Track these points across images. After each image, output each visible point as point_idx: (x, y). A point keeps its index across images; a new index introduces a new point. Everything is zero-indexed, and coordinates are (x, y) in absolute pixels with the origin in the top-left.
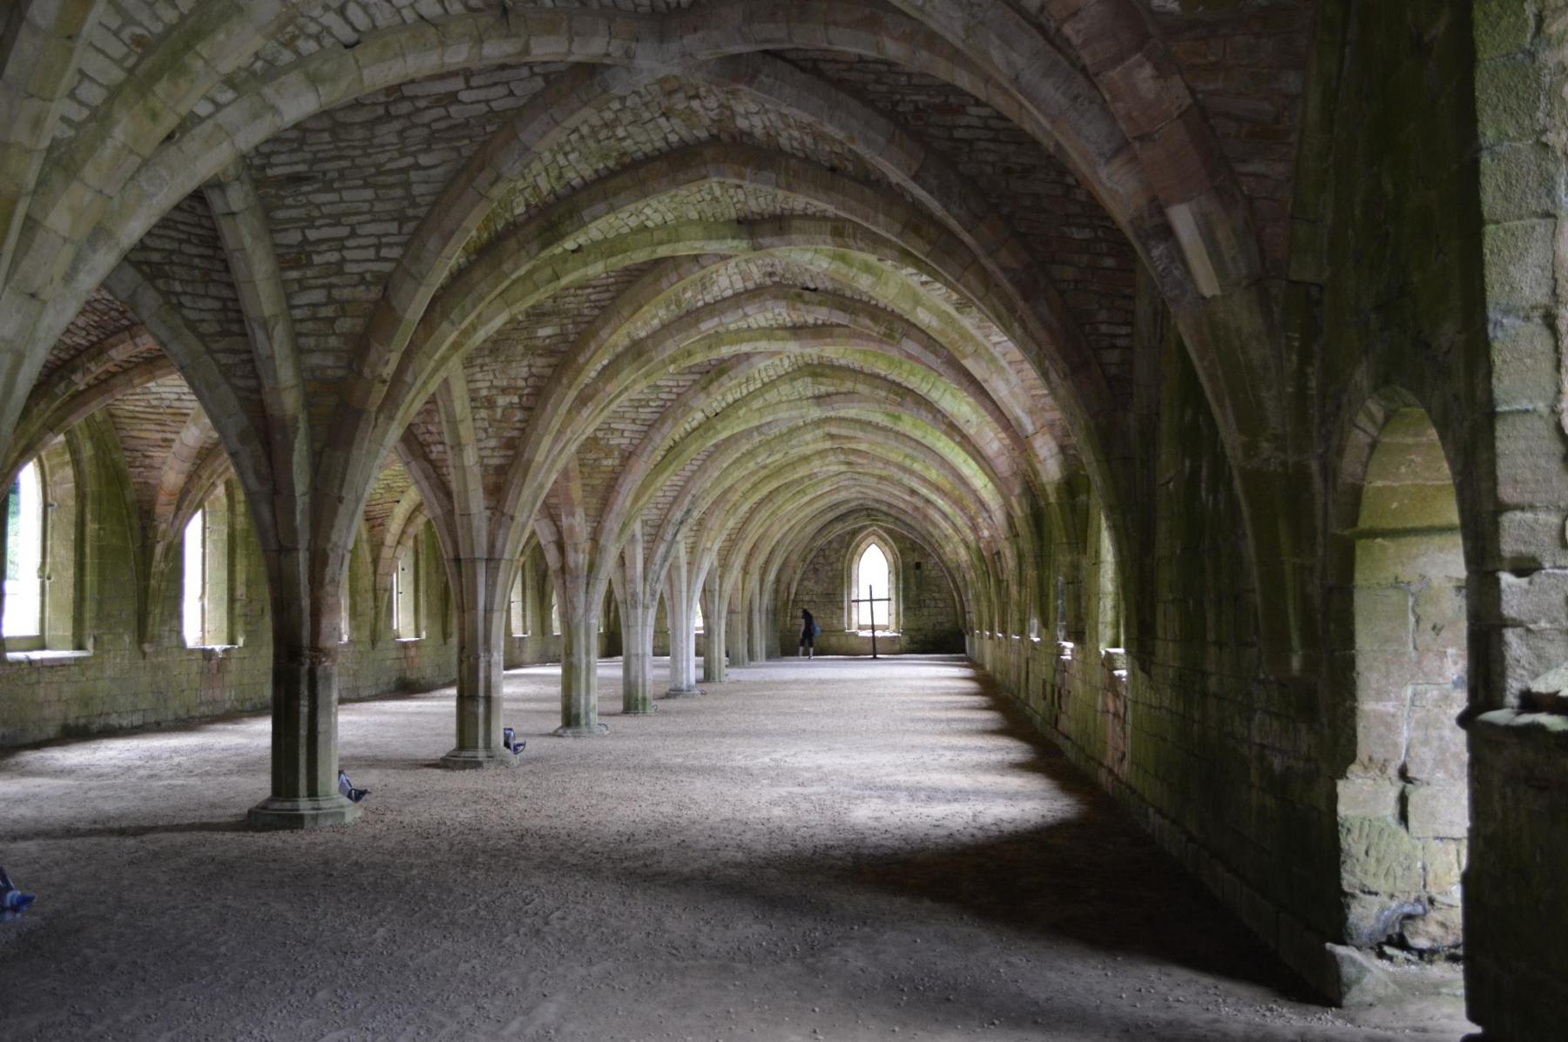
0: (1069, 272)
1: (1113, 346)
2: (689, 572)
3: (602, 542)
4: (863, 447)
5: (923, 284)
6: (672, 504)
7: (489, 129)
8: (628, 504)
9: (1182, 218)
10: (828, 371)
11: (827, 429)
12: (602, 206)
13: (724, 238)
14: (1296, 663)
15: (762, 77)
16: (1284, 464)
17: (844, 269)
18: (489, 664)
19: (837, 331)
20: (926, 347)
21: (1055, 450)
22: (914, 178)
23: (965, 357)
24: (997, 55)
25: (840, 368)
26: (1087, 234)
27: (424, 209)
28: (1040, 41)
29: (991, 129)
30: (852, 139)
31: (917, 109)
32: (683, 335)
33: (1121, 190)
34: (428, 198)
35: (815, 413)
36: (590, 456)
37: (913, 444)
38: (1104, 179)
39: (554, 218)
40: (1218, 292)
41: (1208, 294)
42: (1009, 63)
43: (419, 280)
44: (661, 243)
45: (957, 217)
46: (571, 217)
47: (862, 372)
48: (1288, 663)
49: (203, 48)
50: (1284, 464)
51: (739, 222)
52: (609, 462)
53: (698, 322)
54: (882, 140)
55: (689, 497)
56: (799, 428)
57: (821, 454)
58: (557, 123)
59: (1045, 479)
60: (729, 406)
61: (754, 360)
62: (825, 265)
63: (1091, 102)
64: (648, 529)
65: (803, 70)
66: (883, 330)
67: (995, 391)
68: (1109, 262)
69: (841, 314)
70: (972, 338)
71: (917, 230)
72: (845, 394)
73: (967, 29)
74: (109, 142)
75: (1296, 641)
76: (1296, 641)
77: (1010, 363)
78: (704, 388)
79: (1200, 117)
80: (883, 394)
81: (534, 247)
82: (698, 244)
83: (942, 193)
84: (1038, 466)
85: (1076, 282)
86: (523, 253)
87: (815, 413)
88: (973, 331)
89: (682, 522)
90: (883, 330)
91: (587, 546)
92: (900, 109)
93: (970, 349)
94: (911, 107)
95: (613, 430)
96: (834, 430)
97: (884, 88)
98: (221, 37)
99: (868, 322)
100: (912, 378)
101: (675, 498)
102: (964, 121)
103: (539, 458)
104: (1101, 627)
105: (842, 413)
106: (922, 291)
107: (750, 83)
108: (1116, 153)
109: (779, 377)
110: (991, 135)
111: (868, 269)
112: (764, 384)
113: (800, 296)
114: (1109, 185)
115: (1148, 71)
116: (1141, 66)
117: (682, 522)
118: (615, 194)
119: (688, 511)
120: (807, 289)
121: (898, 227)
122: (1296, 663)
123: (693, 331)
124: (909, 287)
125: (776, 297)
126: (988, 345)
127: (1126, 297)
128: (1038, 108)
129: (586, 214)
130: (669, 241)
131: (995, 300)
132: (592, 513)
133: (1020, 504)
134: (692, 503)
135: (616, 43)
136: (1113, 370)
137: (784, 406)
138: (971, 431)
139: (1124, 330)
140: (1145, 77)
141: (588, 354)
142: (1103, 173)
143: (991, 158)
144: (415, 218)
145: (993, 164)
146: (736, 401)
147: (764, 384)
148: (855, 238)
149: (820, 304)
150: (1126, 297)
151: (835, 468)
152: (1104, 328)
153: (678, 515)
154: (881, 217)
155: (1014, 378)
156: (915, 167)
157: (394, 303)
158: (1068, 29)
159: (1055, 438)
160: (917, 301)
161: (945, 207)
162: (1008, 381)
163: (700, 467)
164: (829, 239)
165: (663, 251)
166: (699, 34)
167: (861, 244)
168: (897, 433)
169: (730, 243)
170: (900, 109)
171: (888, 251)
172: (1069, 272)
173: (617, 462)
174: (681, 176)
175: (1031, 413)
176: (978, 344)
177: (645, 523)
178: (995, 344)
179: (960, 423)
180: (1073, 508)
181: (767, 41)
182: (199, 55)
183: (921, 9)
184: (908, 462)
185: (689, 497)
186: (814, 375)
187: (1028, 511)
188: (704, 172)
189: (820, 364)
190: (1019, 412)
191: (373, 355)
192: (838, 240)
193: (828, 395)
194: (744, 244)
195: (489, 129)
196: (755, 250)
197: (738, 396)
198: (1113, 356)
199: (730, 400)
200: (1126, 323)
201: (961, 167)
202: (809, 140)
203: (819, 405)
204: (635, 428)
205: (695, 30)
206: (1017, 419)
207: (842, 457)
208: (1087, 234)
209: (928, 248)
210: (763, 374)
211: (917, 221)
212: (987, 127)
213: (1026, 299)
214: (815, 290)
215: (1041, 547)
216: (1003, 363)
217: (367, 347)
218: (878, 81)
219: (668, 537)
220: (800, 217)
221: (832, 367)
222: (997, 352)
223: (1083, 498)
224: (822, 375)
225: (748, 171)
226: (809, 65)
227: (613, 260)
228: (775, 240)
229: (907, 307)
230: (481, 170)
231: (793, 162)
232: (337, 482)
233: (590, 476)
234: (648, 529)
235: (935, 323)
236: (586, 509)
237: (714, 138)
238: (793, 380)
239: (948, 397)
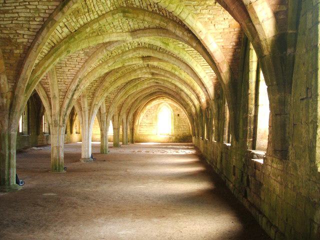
2: (89, 113)
3: (16, 93)
6: (71, 82)
10: (131, 10)
36: (7, 48)
52: (18, 51)
55: (78, 79)
56: (127, 51)
57: (141, 68)
60: (82, 26)
64: (61, 93)
89: (75, 90)
91: (9, 95)
95: (19, 34)
100: (171, 5)
101: (73, 80)
109: (107, 13)
112: (99, 16)
117: (75, 90)
119: (78, 86)
132: (11, 77)
134: (80, 82)
137: (115, 34)
146: (85, 24)
147: (99, 16)
151: (147, 76)
153: (73, 87)
163: (82, 66)
173: (22, 51)
177: (60, 90)
184: (173, 71)
185: (78, 79)
197: (85, 21)
199: (82, 23)
203: (132, 36)
204: (30, 33)
207: (148, 70)
210: (97, 9)
219: (70, 97)
224: (128, 12)
233: (9, 59)
234: (61, 93)
236: (8, 76)
238: (113, 14)
239: (190, 17)
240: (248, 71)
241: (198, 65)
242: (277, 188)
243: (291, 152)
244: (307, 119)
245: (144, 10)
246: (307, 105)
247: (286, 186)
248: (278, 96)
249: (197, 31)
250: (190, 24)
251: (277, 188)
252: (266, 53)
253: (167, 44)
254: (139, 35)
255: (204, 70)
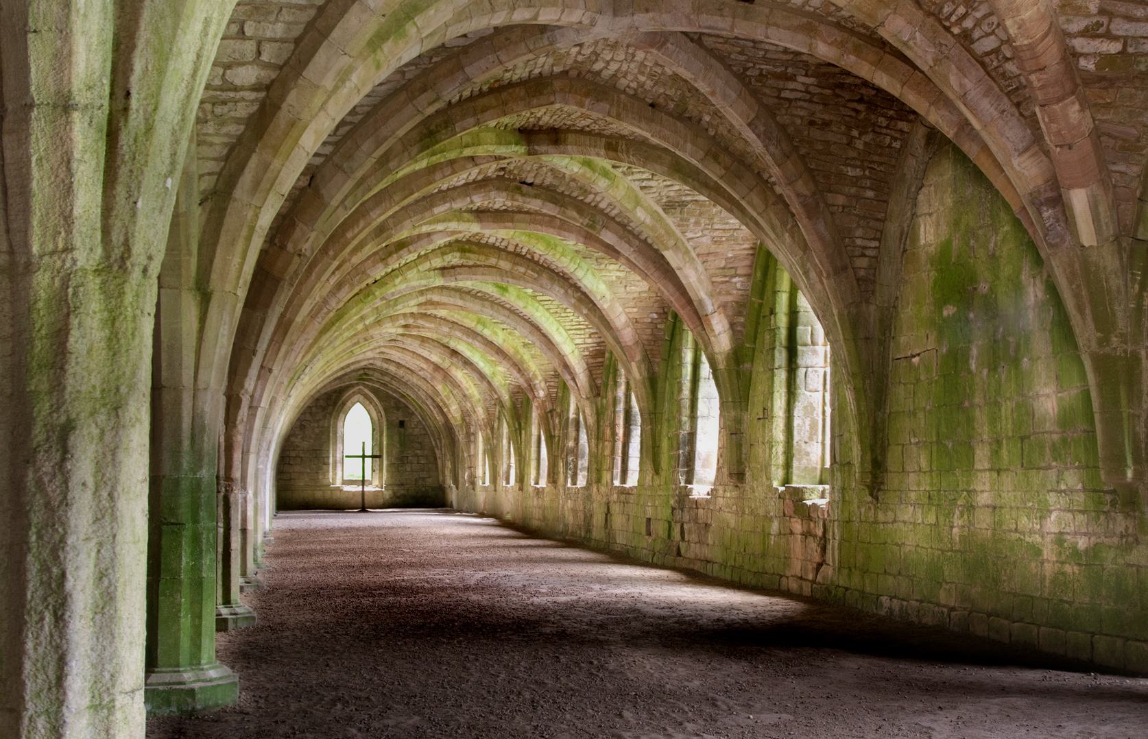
0: (841, 200)
1: (863, 255)
4: (442, 313)
5: (642, 188)
7: (435, 60)
8: (298, 360)
9: (1079, 200)
10: (475, 248)
11: (429, 297)
12: (471, 120)
13: (510, 144)
14: (1130, 474)
15: (669, 45)
16: (1125, 351)
17: (589, 173)
18: (245, 499)
19: (518, 216)
20: (621, 238)
21: (727, 326)
22: (749, 125)
23: (667, 249)
24: (953, 80)
25: (487, 245)
26: (858, 172)
27: (360, 117)
28: (982, 72)
29: (809, 93)
30: (713, 93)
31: (761, 74)
32: (419, 216)
33: (1026, 173)
34: (366, 109)
35: (439, 282)
37: (507, 313)
38: (1016, 165)
39: (433, 127)
40: (1095, 244)
41: (1086, 244)
42: (961, 85)
43: (348, 175)
44: (467, 146)
45: (772, 155)
46: (446, 127)
47: (505, 250)
48: (1124, 474)
49: (419, 20)
50: (1125, 351)
51: (519, 130)
53: (432, 206)
54: (734, 96)
58: (501, 63)
59: (717, 350)
61: (434, 237)
62: (576, 170)
63: (1012, 115)
65: (692, 40)
66: (587, 221)
67: (686, 277)
68: (870, 194)
69: (551, 205)
70: (670, 233)
71: (716, 158)
72: (470, 267)
73: (936, 61)
74: (348, 84)
75: (1129, 461)
76: (1129, 461)
77: (698, 255)
78: (382, 260)
79: (1097, 135)
80: (522, 270)
81: (415, 149)
82: (491, 148)
83: (765, 137)
84: (712, 339)
85: (843, 207)
86: (406, 154)
87: (439, 282)
88: (674, 228)
90: (587, 221)
92: (748, 73)
93: (672, 243)
94: (757, 72)
96: (436, 298)
97: (743, 58)
98: (432, 12)
99: (575, 214)
102: (791, 85)
103: (299, 319)
104: (773, 468)
105: (460, 284)
106: (641, 193)
107: (659, 49)
108: (1026, 150)
110: (808, 97)
111: (605, 174)
113: (519, 189)
114: (1018, 168)
115: (1077, 107)
116: (1073, 103)
118: (483, 111)
120: (524, 183)
121: (701, 154)
122: (1130, 474)
123: (427, 214)
124: (633, 190)
125: (498, 189)
126: (684, 240)
127: (878, 220)
128: (975, 116)
129: (458, 126)
130: (473, 145)
131: (772, 215)
133: (639, 368)
135: (588, 14)
136: (862, 273)
138: (604, 305)
139: (875, 244)
140: (1073, 111)
141: (356, 231)
142: (1015, 162)
143: (802, 113)
144: (351, 123)
145: (802, 118)
148: (628, 152)
149: (536, 197)
150: (878, 220)
152: (859, 242)
154: (689, 145)
155: (700, 268)
156: (753, 116)
157: (323, 191)
158: (1033, 77)
159: (727, 316)
160: (638, 203)
161: (766, 147)
162: (696, 269)
164: (603, 152)
165: (468, 152)
166: (651, 15)
167: (632, 159)
168: (502, 306)
169: (514, 148)
170: (748, 73)
171: (658, 167)
172: (841, 200)
174: (535, 101)
175: (711, 296)
176: (677, 239)
178: (689, 240)
179: (596, 298)
180: (738, 373)
181: (709, 28)
182: (415, 23)
183: (905, 44)
186: (463, 251)
187: (645, 374)
188: (552, 99)
189: (469, 242)
190: (703, 295)
191: (297, 233)
192: (611, 154)
193: (453, 267)
194: (522, 149)
195: (435, 60)
196: (529, 154)
198: (863, 263)
200: (874, 239)
201: (778, 118)
202: (649, 84)
203: (443, 275)
205: (647, 11)
206: (700, 301)
208: (858, 172)
209: (723, 172)
211: (720, 148)
212: (807, 92)
213: (809, 218)
214: (531, 184)
215: (655, 406)
216: (694, 255)
217: (293, 226)
218: (741, 53)
220: (576, 131)
221: (478, 244)
222: (689, 245)
223: (747, 365)
224: (470, 251)
225: (587, 102)
226: (696, 37)
227: (434, 158)
228: (551, 148)
229: (629, 206)
230: (424, 90)
231: (623, 96)
232: (254, 338)
235: (648, 221)
237: (565, 73)
238: (443, 254)
239: (589, 276)
240: (681, 365)
241: (561, 330)
242: (732, 519)
243: (748, 474)
244: (764, 437)
245: (498, 248)
246: (764, 426)
247: (744, 513)
248: (733, 413)
249: (599, 297)
250: (589, 286)
251: (732, 519)
252: (721, 366)
253: (505, 290)
254: (459, 277)
255: (572, 339)
